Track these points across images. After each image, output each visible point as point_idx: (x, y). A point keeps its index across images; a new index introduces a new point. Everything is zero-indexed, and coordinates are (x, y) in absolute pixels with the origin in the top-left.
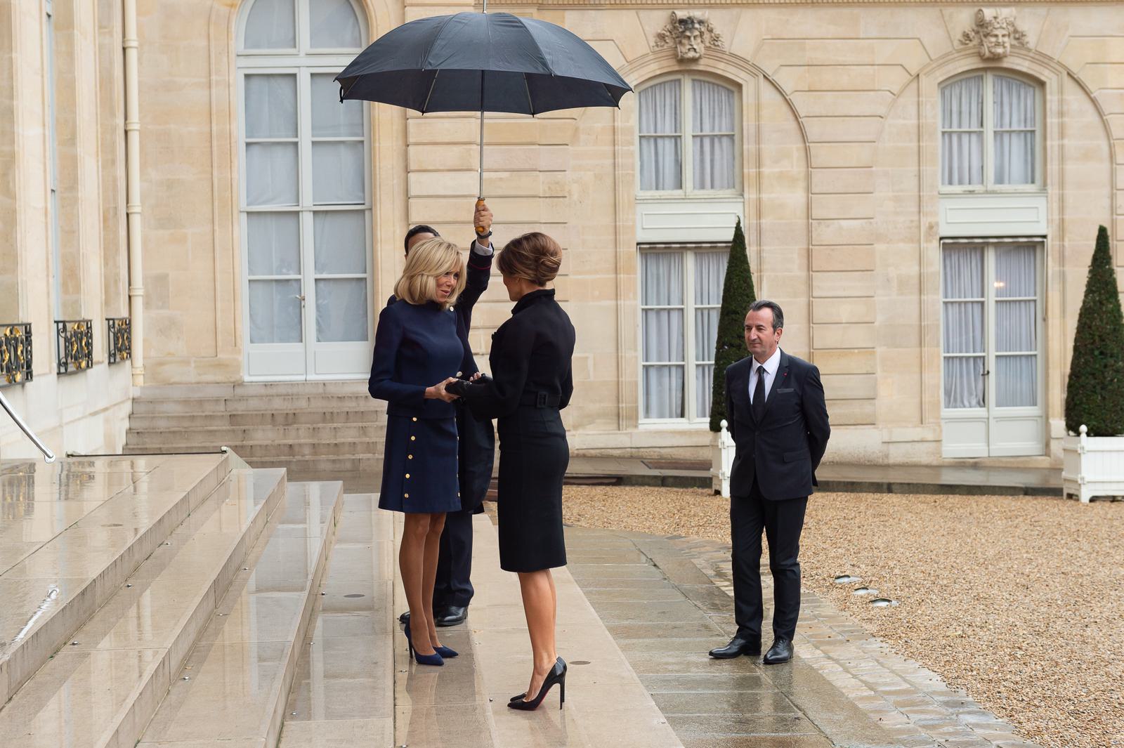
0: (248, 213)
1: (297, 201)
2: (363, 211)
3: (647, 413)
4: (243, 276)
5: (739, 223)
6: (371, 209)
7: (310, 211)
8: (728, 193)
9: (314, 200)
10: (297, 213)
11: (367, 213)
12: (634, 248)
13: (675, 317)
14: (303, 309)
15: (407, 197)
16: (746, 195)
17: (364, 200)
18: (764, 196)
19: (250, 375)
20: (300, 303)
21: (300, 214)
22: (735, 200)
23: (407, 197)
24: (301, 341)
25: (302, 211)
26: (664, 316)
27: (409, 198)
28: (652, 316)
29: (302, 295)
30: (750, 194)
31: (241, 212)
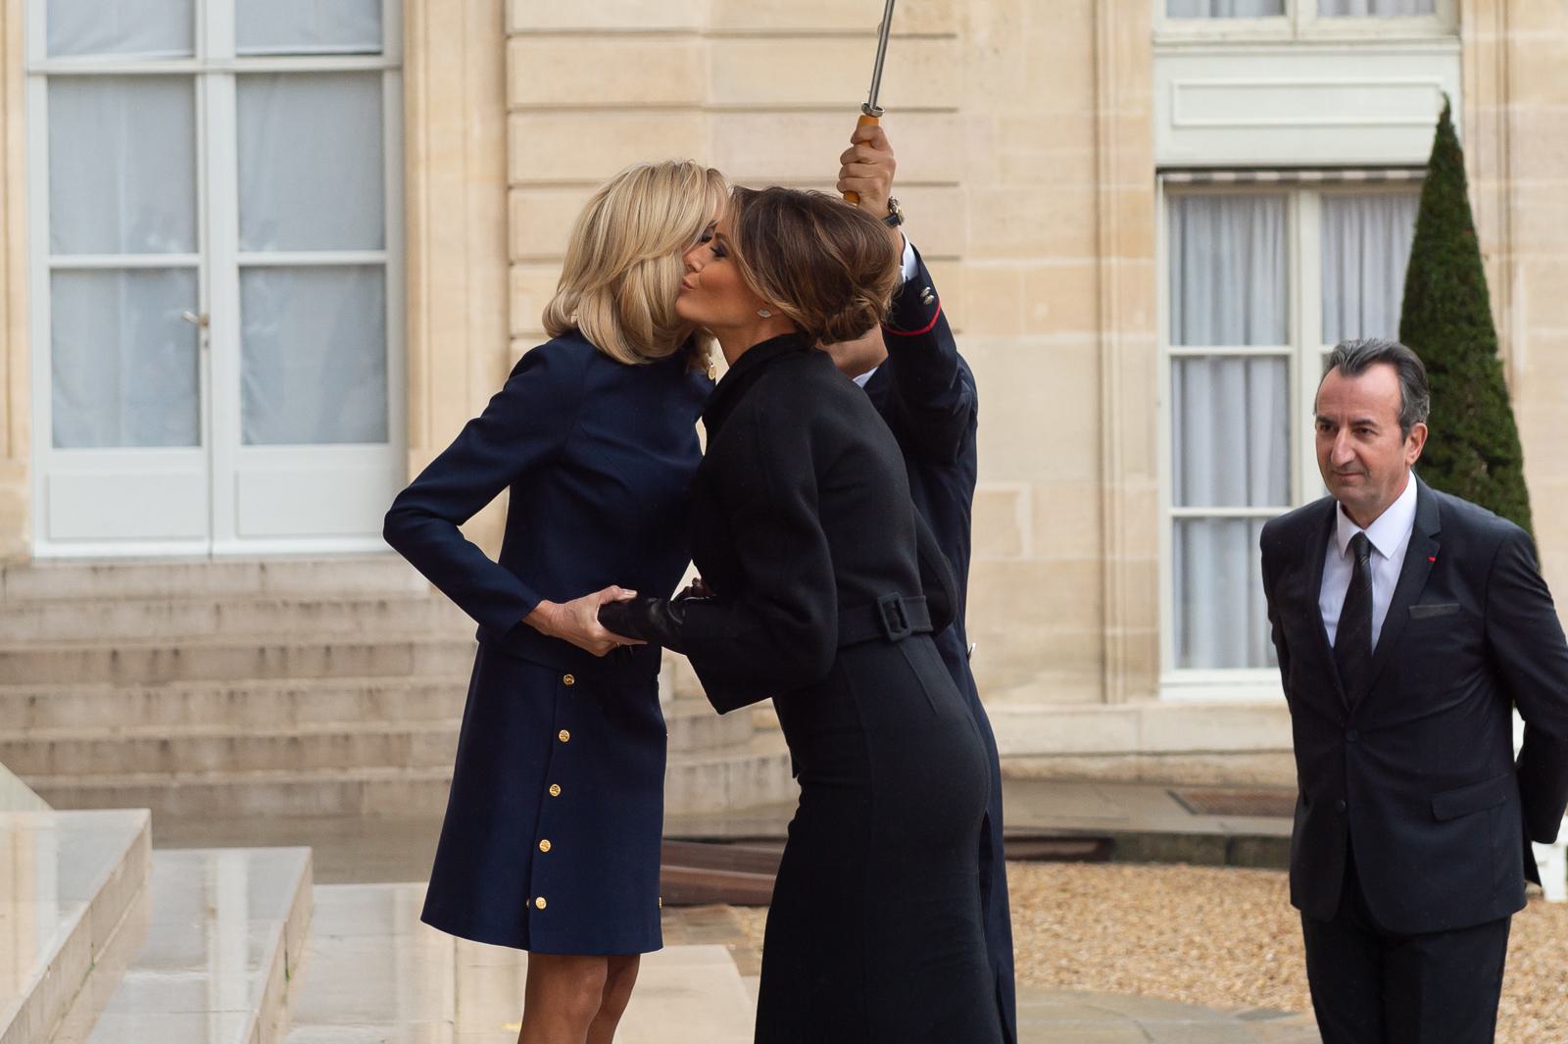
0: (53, 79)
1: (190, 43)
2: (376, 75)
3: (1186, 653)
4: (34, 257)
5: (1446, 114)
6: (399, 69)
7: (226, 73)
8: (1418, 26)
9: (239, 40)
10: (188, 79)
11: (389, 81)
12: (1147, 183)
13: (1265, 379)
14: (203, 354)
15: (504, 35)
16: (1467, 34)
17: (380, 39)
18: (1520, 36)
19: (50, 540)
20: (194, 335)
21: (200, 83)
22: (1435, 47)
23: (504, 35)
24: (197, 442)
25: (204, 74)
26: (1235, 375)
27: (509, 37)
28: (1200, 377)
29: (203, 310)
30: (1480, 32)
31: (30, 74)
